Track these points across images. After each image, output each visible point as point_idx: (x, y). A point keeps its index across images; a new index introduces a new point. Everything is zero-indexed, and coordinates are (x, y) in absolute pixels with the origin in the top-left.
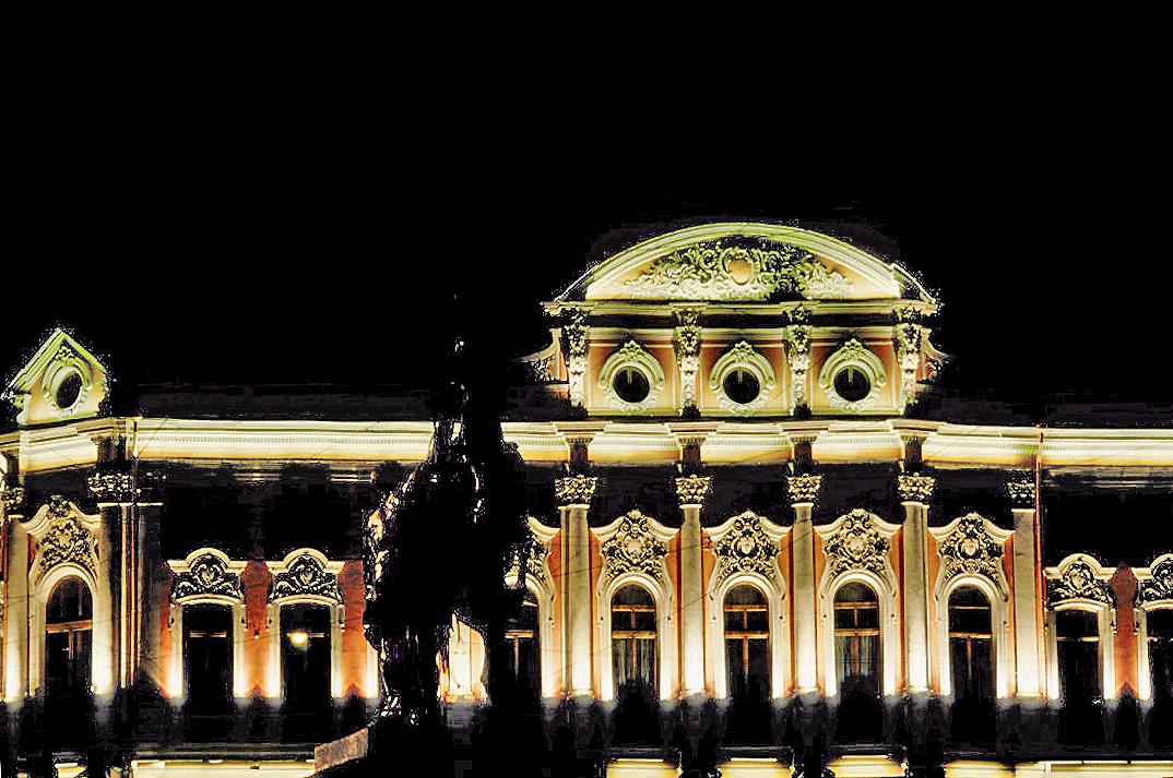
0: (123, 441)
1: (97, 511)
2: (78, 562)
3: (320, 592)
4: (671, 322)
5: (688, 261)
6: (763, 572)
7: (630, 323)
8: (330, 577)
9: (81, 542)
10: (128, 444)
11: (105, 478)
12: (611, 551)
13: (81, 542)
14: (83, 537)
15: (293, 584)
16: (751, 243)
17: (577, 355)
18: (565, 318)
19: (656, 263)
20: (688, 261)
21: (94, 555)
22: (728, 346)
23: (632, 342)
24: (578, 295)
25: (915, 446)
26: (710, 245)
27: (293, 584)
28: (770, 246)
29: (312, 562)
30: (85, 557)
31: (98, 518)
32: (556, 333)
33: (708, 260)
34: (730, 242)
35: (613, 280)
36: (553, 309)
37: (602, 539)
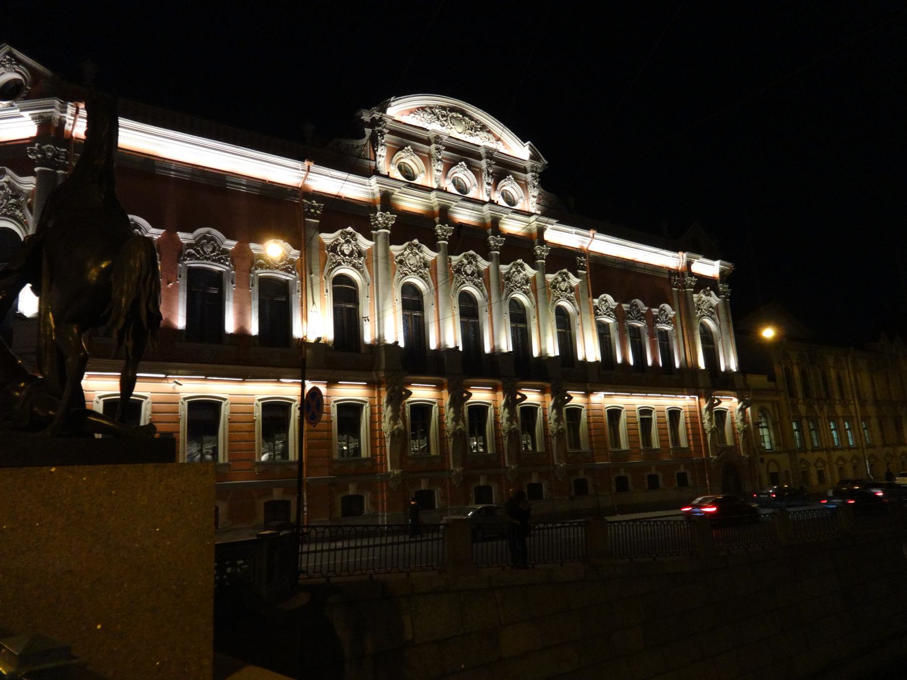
0: (62, 123)
1: (33, 174)
2: (10, 216)
3: (218, 261)
4: (428, 142)
5: (433, 113)
6: (477, 285)
7: (406, 138)
8: (225, 252)
9: (13, 201)
10: (68, 127)
11: (44, 147)
12: (401, 262)
13: (13, 201)
14: (16, 197)
15: (198, 252)
16: (464, 113)
17: (382, 145)
18: (374, 123)
19: (418, 109)
20: (433, 113)
21: (27, 211)
22: (454, 163)
23: (409, 147)
24: (385, 112)
25: (541, 231)
26: (444, 108)
27: (198, 252)
28: (471, 118)
29: (212, 239)
30: (18, 212)
31: (32, 179)
32: (368, 131)
33: (443, 116)
34: (453, 109)
35: (402, 111)
36: (366, 117)
37: (396, 254)
